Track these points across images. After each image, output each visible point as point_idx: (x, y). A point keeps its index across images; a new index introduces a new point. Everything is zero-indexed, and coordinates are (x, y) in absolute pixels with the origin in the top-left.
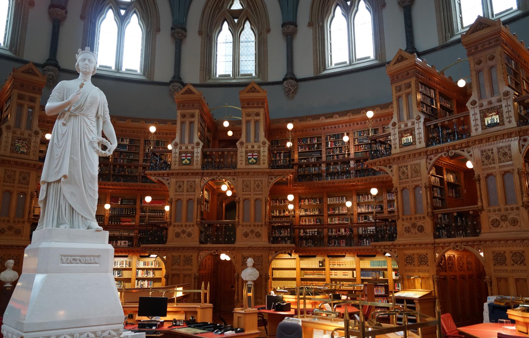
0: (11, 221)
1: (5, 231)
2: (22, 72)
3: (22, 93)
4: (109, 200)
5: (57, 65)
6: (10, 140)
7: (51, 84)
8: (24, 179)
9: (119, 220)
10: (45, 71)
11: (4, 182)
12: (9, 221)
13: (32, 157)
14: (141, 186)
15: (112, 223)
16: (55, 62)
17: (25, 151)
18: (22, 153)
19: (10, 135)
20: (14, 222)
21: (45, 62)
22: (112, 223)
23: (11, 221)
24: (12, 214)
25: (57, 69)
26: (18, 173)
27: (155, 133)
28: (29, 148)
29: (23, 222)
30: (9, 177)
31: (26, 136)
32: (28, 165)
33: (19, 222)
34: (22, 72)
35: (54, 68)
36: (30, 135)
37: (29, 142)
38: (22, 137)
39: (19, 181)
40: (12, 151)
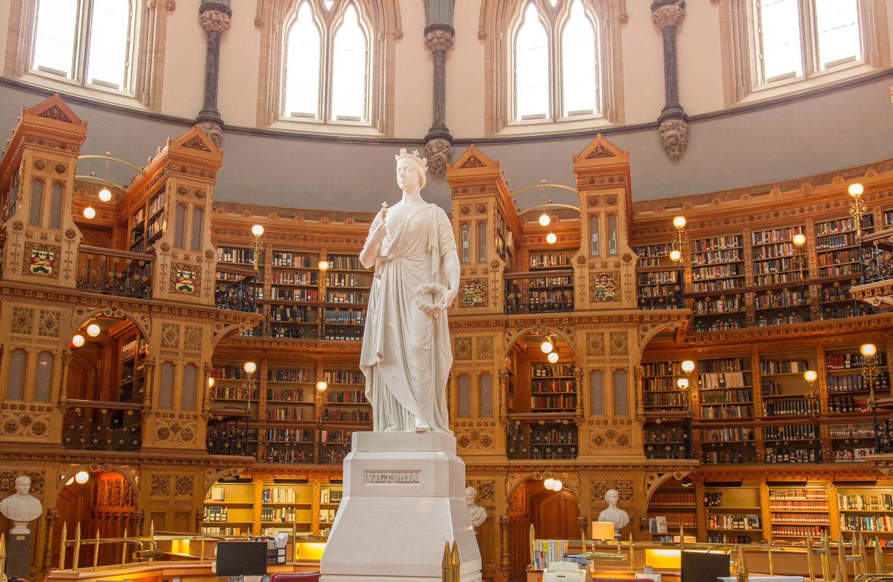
0: (610, 422)
1: (602, 440)
2: (588, 157)
3: (594, 193)
4: (823, 360)
5: (680, 115)
6: (586, 281)
7: (677, 153)
8: (619, 345)
9: (853, 401)
10: (663, 132)
11: (589, 355)
12: (606, 423)
13: (625, 303)
14: (805, 330)
15: (834, 410)
16: (675, 110)
17: (612, 294)
18: (610, 299)
19: (586, 271)
20: (615, 423)
21: (659, 114)
22: (834, 410)
23: (610, 422)
24: (609, 410)
25: (681, 121)
26: (607, 337)
27: (686, 227)
28: (619, 287)
29: (630, 422)
30: (595, 345)
31: (611, 267)
32: (620, 319)
33: (622, 423)
34: (588, 157)
35: (675, 121)
36: (617, 266)
37: (618, 277)
38: (604, 271)
39: (612, 350)
40: (593, 300)
